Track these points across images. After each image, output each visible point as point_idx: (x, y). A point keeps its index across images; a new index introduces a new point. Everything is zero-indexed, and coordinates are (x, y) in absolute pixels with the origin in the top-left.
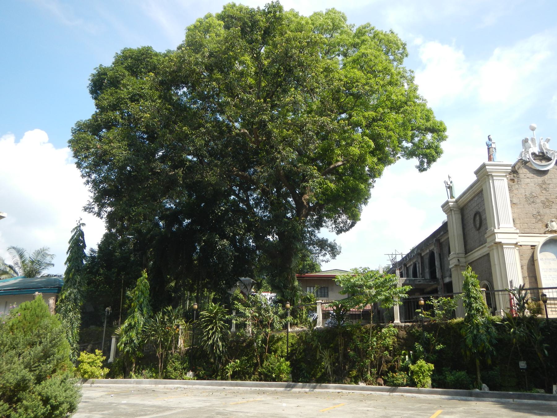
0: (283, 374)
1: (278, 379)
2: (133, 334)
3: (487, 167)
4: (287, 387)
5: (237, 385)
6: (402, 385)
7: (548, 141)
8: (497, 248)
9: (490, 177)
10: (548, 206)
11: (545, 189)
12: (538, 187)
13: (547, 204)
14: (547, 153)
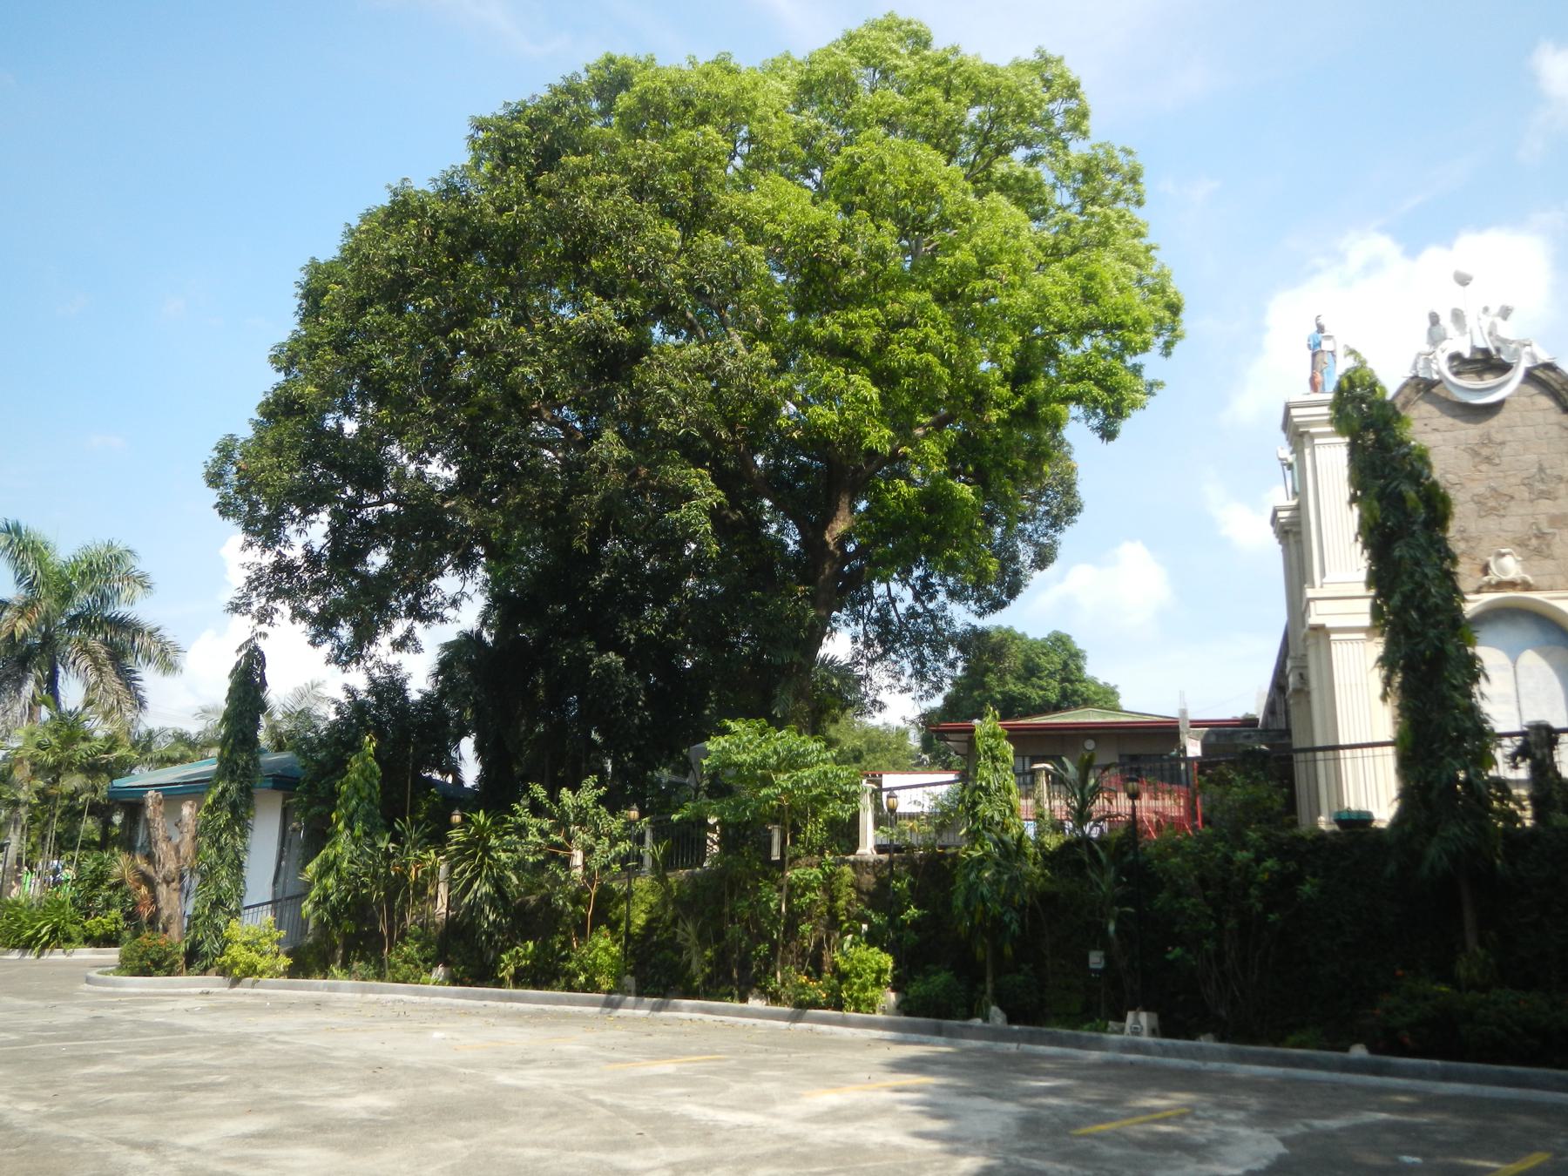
0: (601, 974)
1: (590, 986)
2: (330, 881)
3: (1294, 412)
4: (609, 1004)
5: (482, 997)
6: (814, 1004)
7: (1505, 313)
8: (1318, 643)
9: (1306, 439)
10: (1494, 509)
11: (1488, 459)
12: (1466, 456)
13: (1492, 503)
14: (1498, 350)
